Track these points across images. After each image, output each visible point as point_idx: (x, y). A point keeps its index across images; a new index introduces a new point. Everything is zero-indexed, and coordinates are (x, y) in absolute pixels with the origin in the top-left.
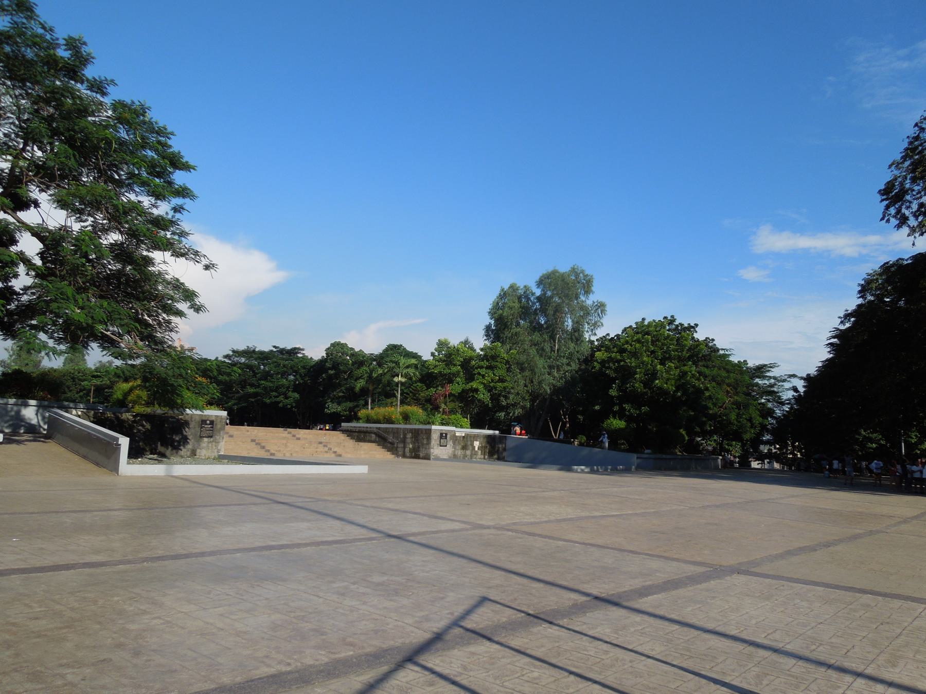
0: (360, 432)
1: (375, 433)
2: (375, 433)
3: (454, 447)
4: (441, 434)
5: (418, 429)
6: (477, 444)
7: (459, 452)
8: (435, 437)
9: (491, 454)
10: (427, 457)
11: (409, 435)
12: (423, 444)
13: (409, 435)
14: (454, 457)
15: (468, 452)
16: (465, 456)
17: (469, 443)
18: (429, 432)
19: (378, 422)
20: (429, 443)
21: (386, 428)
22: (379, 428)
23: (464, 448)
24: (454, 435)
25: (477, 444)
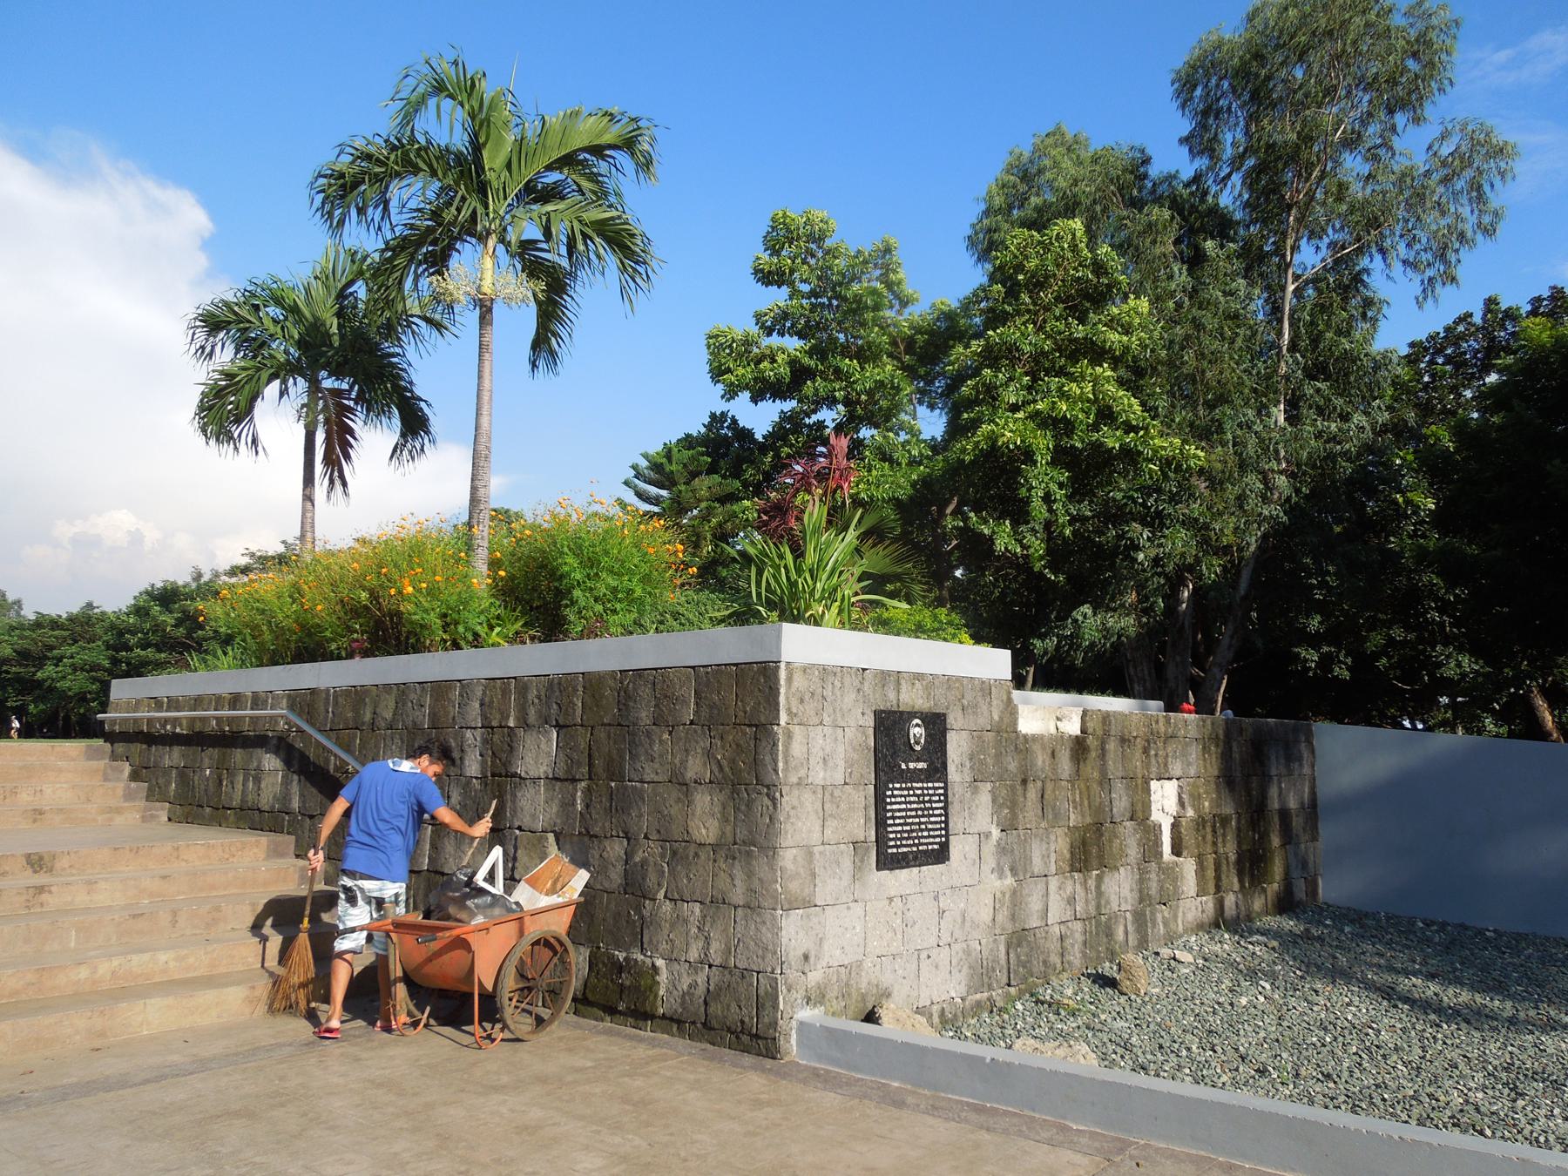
0: (197, 739)
1: (284, 747)
2: (284, 747)
3: (1014, 862)
4: (889, 725)
5: (628, 683)
6: (1165, 800)
7: (1055, 903)
8: (821, 756)
9: (1252, 865)
10: (737, 1024)
11: (538, 755)
12: (679, 850)
13: (538, 755)
14: (1018, 975)
15: (1120, 888)
16: (1100, 927)
17: (1121, 802)
18: (742, 709)
19: (309, 648)
20: (750, 837)
21: (357, 695)
22: (305, 702)
23: (1088, 854)
24: (1006, 734)
25: (1165, 800)
